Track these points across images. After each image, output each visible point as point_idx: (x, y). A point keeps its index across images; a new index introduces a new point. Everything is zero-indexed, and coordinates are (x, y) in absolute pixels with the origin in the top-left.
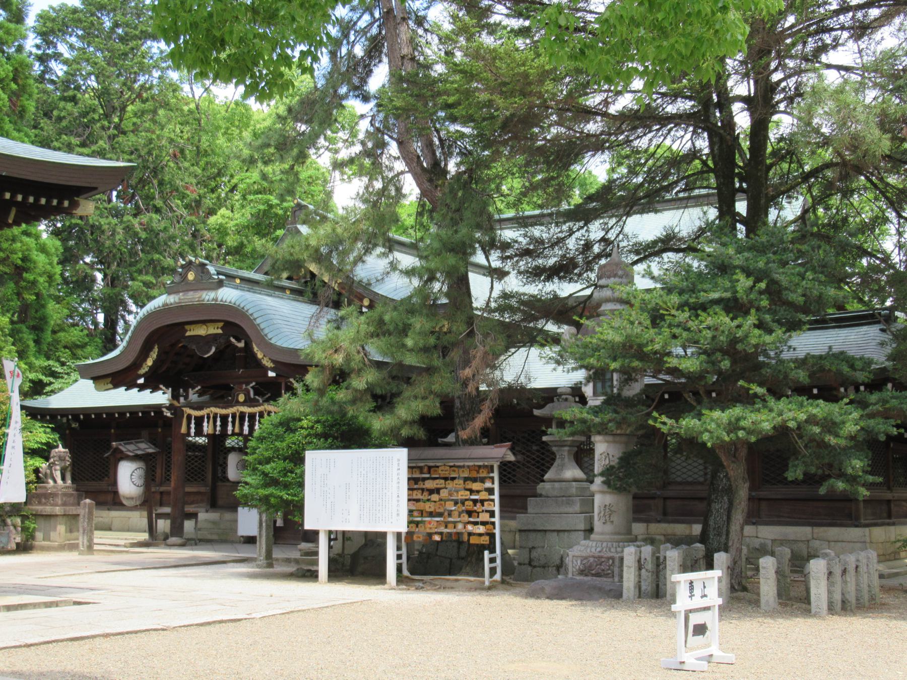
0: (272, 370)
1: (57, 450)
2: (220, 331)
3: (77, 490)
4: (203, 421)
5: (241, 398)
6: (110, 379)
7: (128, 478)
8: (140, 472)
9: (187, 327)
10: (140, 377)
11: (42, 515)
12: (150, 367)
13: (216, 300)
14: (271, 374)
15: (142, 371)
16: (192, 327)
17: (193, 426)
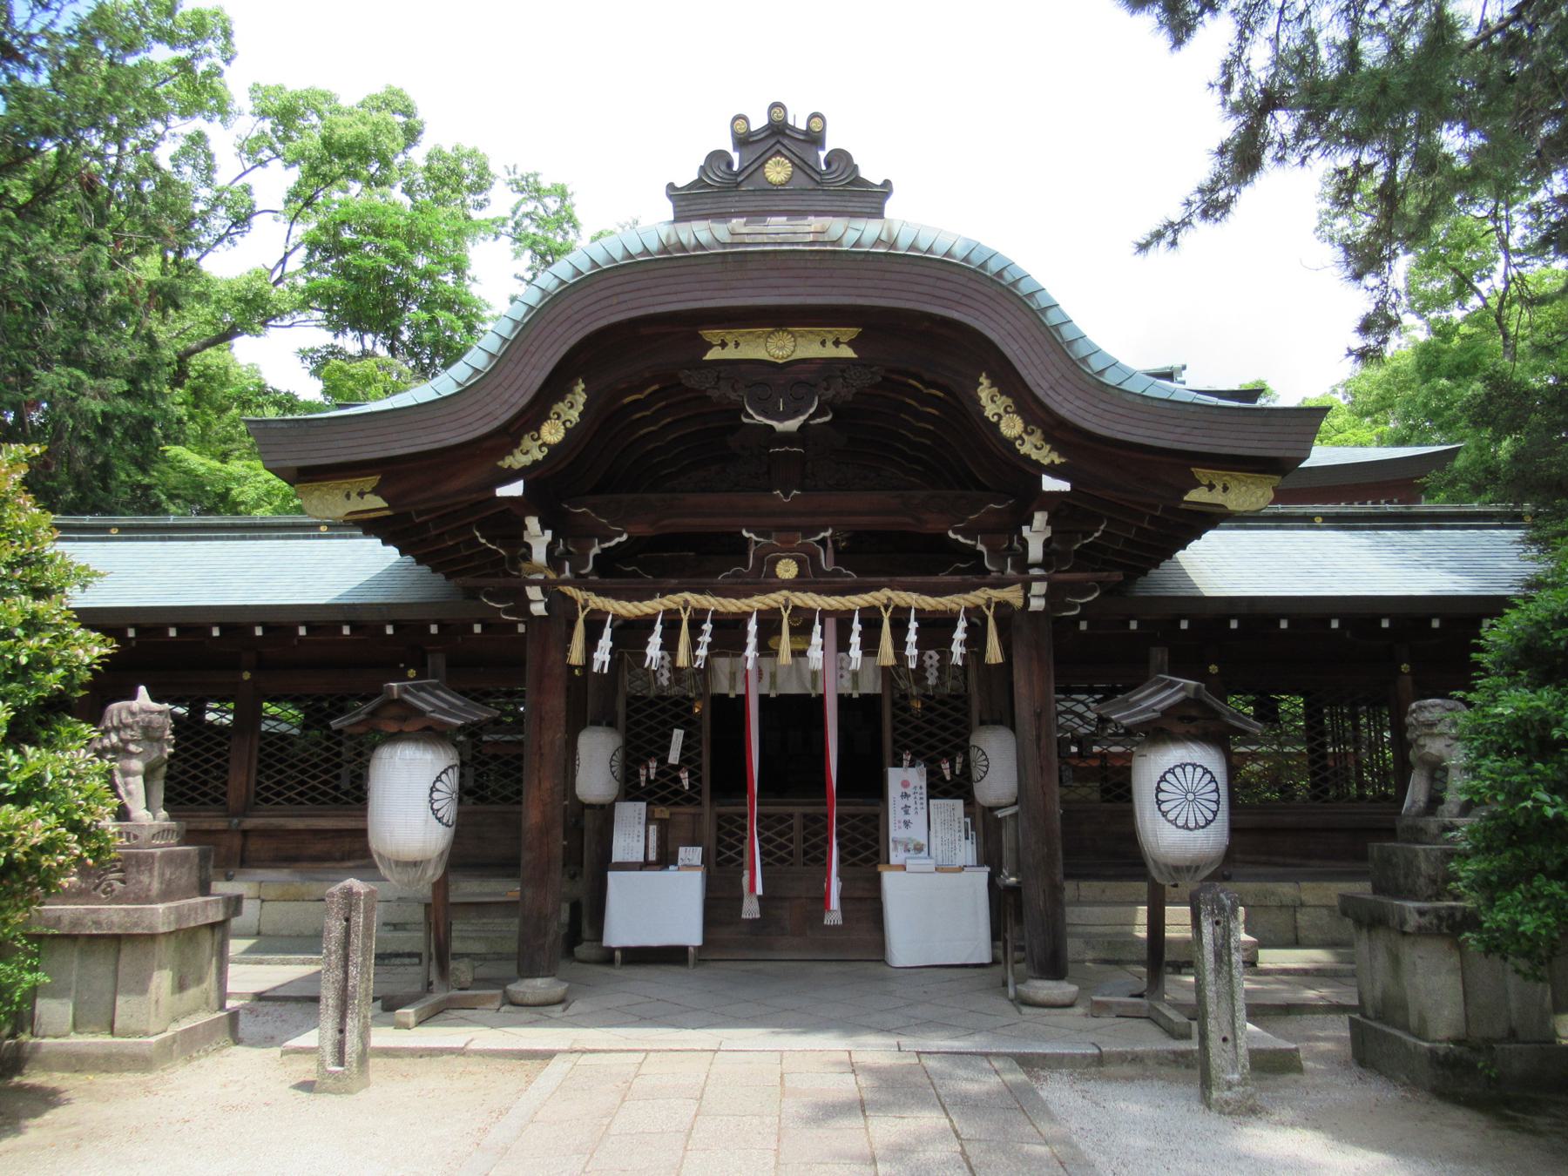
0: (1055, 471)
1: (135, 705)
2: (847, 352)
3: (188, 837)
4: (651, 630)
5: (787, 569)
6: (374, 480)
7: (410, 798)
8: (451, 782)
9: (710, 335)
10: (509, 476)
11: (72, 938)
12: (554, 449)
13: (893, 245)
14: (1050, 484)
15: (518, 460)
16: (730, 336)
17: (605, 643)
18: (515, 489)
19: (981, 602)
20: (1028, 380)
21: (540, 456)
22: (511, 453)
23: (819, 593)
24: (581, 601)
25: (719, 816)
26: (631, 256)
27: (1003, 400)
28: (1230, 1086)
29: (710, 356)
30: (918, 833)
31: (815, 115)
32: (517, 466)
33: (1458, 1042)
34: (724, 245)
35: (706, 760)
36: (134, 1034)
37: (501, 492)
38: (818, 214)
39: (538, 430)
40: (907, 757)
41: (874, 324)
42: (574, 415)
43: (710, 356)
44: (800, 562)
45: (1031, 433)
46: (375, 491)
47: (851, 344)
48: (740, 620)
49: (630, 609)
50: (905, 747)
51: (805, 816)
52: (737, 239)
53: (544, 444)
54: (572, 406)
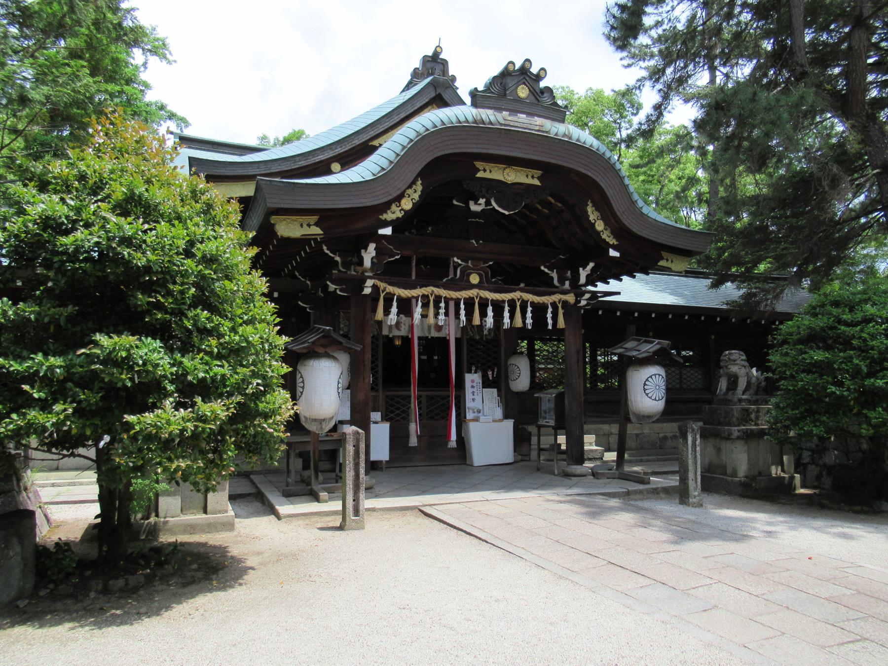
0: (615, 248)
2: (537, 182)
5: (474, 279)
6: (314, 219)
9: (479, 164)
10: (385, 224)
14: (613, 253)
15: (389, 216)
16: (488, 166)
18: (387, 231)
19: (557, 300)
20: (615, 207)
21: (400, 216)
22: (386, 212)
23: (491, 291)
24: (382, 288)
25: (387, 396)
26: (460, 122)
27: (597, 214)
28: (695, 497)
29: (478, 175)
30: (478, 404)
31: (543, 69)
32: (389, 219)
33: (746, 477)
34: (501, 124)
35: (380, 369)
36: (220, 512)
37: (381, 232)
38: (539, 116)
39: (400, 202)
40: (474, 368)
41: (547, 170)
42: (416, 196)
43: (478, 175)
44: (480, 276)
45: (606, 230)
46: (317, 224)
47: (538, 178)
48: (457, 302)
49: (405, 293)
50: (472, 364)
51: (427, 396)
52: (507, 123)
53: (402, 209)
54: (415, 191)
